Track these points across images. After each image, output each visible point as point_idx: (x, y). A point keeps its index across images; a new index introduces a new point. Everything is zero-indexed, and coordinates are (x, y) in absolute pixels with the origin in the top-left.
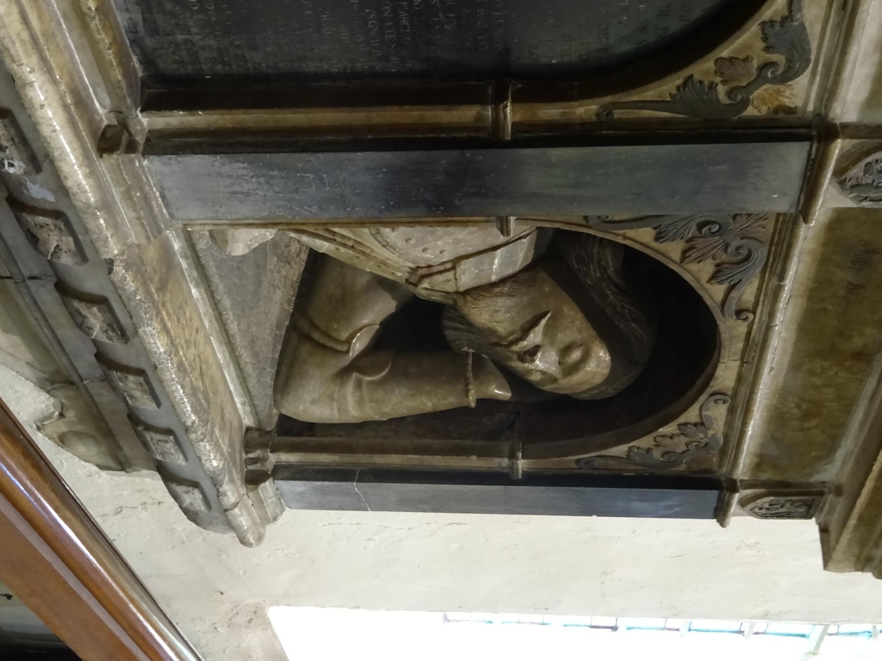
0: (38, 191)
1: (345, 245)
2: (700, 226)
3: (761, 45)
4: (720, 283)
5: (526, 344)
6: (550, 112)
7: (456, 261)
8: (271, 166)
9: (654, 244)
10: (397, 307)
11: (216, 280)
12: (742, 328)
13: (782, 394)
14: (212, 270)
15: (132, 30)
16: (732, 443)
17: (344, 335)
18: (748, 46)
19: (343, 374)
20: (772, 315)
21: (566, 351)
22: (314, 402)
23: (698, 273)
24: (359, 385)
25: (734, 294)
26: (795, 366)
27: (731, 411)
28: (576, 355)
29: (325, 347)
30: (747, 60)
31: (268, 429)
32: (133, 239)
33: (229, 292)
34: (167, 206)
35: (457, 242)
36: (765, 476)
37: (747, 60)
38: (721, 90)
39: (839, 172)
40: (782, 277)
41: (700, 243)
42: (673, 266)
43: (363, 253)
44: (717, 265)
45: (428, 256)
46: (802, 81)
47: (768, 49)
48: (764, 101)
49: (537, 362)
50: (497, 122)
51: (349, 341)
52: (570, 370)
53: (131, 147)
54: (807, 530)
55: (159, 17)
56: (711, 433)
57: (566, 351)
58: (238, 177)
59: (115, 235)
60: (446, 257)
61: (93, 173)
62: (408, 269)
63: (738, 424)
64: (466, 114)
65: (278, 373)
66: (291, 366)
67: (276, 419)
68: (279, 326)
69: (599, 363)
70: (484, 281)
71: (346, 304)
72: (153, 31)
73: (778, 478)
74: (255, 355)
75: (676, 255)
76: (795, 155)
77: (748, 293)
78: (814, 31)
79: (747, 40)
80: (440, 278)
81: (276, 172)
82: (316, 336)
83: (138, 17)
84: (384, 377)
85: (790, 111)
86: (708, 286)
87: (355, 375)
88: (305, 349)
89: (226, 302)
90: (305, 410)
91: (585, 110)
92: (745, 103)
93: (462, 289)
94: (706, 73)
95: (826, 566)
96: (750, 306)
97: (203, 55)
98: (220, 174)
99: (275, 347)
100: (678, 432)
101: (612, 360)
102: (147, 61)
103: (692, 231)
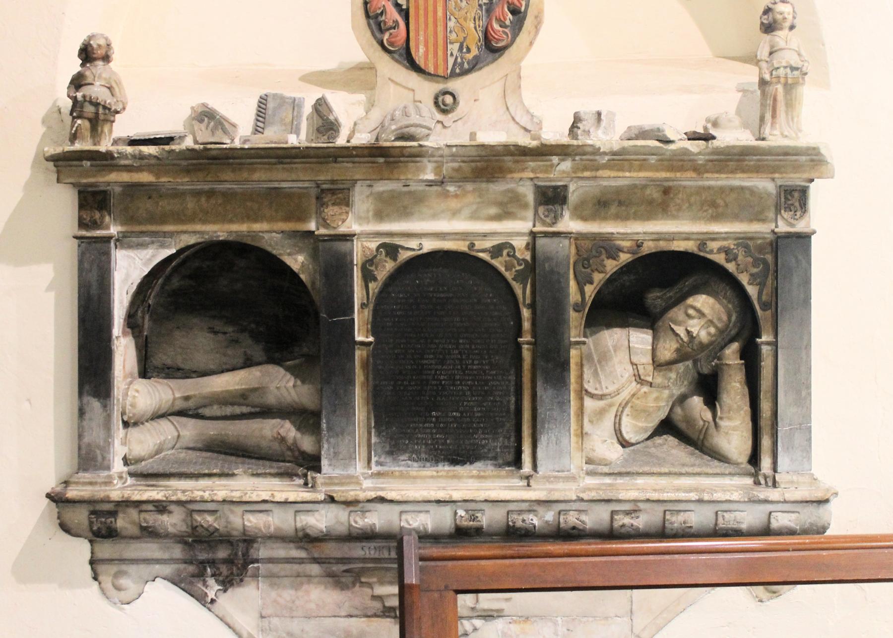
0: (549, 516)
1: (622, 412)
2: (585, 268)
3: (500, 258)
4: (618, 256)
5: (683, 334)
6: (526, 325)
7: (632, 363)
8: (543, 427)
9: (595, 284)
10: (700, 396)
11: (628, 470)
12: (651, 244)
13: (695, 219)
14: (623, 470)
15: (495, 465)
16: (742, 235)
17: (701, 423)
18: (501, 263)
19: (716, 426)
20: (637, 233)
21: (689, 317)
22: (729, 443)
23: (611, 266)
24: (721, 418)
25: (625, 250)
26: (674, 217)
27: (713, 239)
28: (691, 312)
29: (705, 433)
30: (506, 261)
31: (753, 471)
32: (574, 488)
33: (641, 466)
34: (563, 471)
35: (620, 362)
36: (771, 214)
37: (506, 261)
38: (518, 268)
39: (551, 225)
40: (613, 234)
41: (594, 267)
42: (608, 276)
43: (626, 404)
44: (608, 258)
45: (627, 375)
46: (514, 243)
47: (502, 256)
48: (523, 254)
49: (692, 330)
50: (528, 343)
51: (704, 421)
52: (701, 314)
53: (531, 476)
54: (815, 190)
55: (490, 456)
56: (732, 247)
57: (689, 317)
58: (548, 440)
59: (566, 491)
60: (630, 368)
61: (535, 490)
62: (639, 386)
63: (723, 235)
64: (527, 354)
65: (720, 460)
66: (715, 452)
67: (749, 467)
68: (692, 454)
69: (702, 301)
70: (650, 353)
71: (689, 420)
72: (495, 458)
73: (773, 209)
74: (693, 465)
75: (601, 276)
76: (541, 242)
77: (626, 244)
78: (495, 243)
79: (498, 263)
80: (641, 372)
81: (546, 426)
82: (701, 437)
83: (489, 462)
84: (720, 405)
85: (528, 244)
86: (621, 261)
87: (717, 420)
88: (706, 443)
89: (646, 469)
90: (736, 448)
91: (526, 313)
92: (524, 260)
93: (651, 362)
94: (511, 274)
95: (832, 177)
96: (634, 243)
97: (506, 443)
98: (547, 447)
99: (702, 459)
100: (734, 263)
101: (708, 294)
102: (509, 464)
103: (588, 270)
